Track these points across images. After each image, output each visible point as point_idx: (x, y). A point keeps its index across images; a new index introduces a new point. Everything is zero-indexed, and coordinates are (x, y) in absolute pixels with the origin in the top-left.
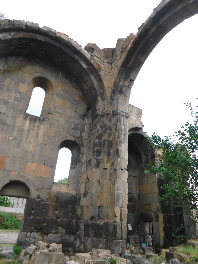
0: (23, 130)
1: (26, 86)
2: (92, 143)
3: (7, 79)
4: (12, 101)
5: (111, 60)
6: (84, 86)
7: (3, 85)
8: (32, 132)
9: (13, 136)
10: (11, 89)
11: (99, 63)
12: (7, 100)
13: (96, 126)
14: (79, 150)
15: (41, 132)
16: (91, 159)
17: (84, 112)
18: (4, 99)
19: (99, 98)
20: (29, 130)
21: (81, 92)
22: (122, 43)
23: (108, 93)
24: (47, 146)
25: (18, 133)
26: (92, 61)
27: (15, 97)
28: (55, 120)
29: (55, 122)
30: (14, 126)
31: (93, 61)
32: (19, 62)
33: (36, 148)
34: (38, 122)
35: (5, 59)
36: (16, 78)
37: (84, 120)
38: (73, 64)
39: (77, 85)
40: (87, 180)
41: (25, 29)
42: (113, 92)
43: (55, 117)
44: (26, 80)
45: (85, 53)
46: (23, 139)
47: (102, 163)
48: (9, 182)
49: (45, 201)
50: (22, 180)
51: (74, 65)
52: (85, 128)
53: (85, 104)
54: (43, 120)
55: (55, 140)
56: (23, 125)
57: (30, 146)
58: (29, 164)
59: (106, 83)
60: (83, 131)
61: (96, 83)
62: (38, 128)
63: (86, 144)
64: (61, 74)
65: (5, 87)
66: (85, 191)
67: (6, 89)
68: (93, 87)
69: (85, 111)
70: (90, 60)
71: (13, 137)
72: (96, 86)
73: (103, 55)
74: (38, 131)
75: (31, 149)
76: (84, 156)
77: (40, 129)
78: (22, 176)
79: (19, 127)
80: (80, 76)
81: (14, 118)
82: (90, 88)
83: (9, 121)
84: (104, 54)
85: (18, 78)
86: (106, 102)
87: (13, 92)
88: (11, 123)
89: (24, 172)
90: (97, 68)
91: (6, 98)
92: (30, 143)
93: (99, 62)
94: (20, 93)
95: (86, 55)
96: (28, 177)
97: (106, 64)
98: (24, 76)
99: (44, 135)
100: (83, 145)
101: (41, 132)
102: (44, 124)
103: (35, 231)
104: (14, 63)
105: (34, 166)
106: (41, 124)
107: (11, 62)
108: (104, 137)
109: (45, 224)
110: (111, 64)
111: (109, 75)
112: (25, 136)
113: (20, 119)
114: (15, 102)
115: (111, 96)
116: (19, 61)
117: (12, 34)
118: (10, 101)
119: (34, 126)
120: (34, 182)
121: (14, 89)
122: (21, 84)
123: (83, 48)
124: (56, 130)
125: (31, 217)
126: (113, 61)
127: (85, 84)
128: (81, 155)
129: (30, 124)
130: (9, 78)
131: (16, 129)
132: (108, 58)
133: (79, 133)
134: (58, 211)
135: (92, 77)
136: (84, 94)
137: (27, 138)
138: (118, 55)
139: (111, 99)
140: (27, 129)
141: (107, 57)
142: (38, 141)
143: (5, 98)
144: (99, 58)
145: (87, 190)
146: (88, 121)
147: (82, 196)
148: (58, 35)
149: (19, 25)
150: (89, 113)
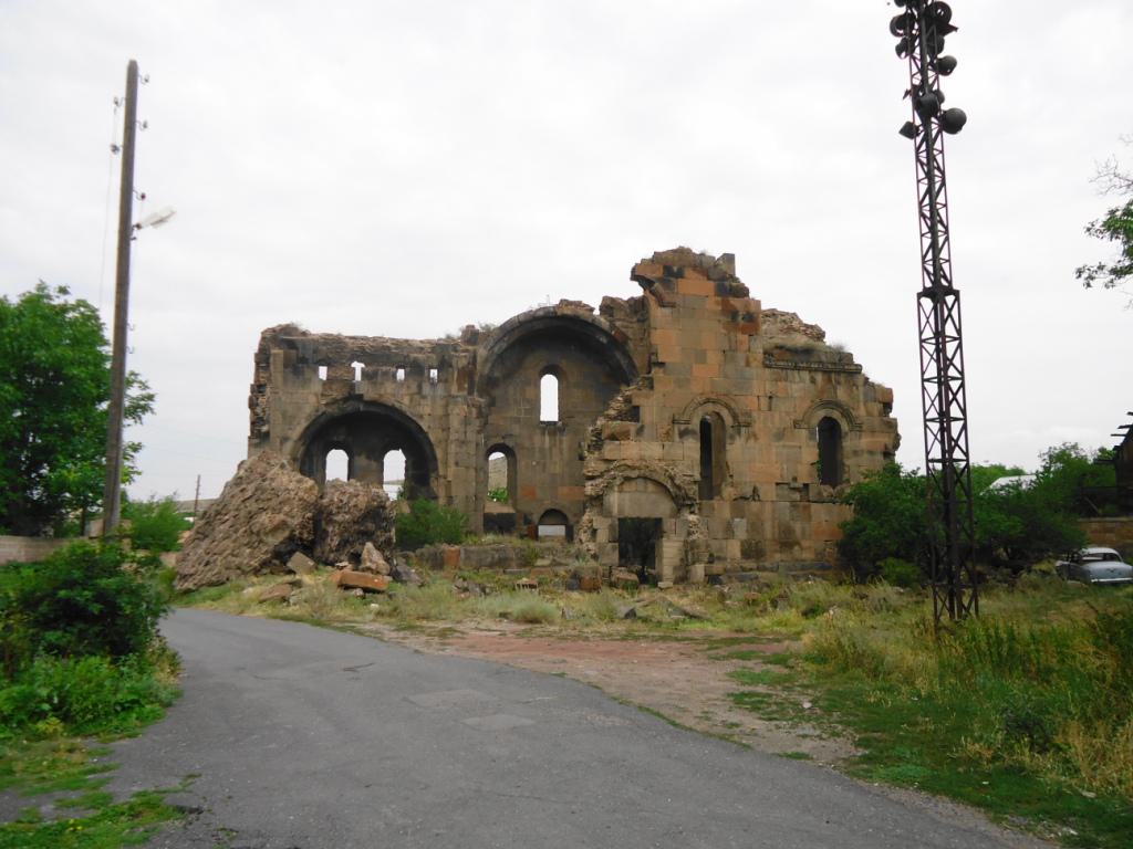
5: (642, 315)
11: (624, 330)
15: (565, 446)
20: (551, 449)
30: (533, 448)
45: (600, 322)
50: (557, 507)
56: (543, 442)
61: (624, 362)
62: (561, 442)
64: (573, 347)
68: (620, 367)
72: (625, 367)
75: (558, 469)
83: (527, 444)
92: (555, 463)
97: (635, 325)
101: (565, 446)
105: (564, 490)
117: (506, 339)
123: (597, 312)
135: (618, 355)
137: (551, 458)
141: (636, 312)
144: (624, 320)
148: (559, 313)
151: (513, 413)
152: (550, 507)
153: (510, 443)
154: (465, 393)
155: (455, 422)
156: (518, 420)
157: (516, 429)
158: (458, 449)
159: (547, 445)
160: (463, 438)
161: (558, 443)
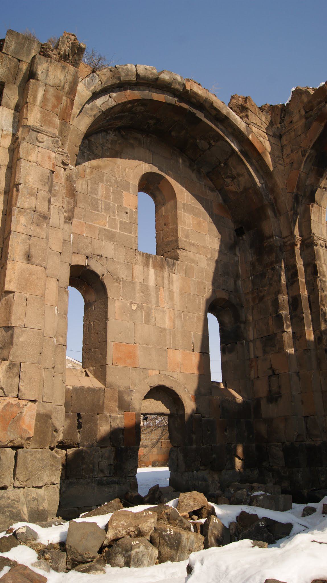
0: (147, 287)
1: (132, 195)
2: (269, 303)
3: (101, 185)
4: (118, 231)
6: (228, 185)
7: (97, 199)
8: (162, 289)
9: (138, 303)
10: (111, 205)
11: (261, 139)
12: (111, 229)
13: (273, 269)
14: (237, 318)
15: (176, 287)
16: (275, 332)
17: (232, 236)
18: (105, 230)
19: (270, 212)
20: (157, 287)
21: (219, 195)
22: (305, 99)
23: (285, 200)
24: (190, 314)
25: (142, 294)
26: (250, 137)
27: (121, 222)
28: (193, 261)
29: (193, 264)
30: (133, 283)
31: (252, 136)
32: (110, 146)
33: (174, 320)
34: (167, 268)
35: (87, 142)
36: (113, 182)
37: (235, 254)
38: (212, 141)
39: (211, 180)
40: (270, 372)
41: (134, 82)
42: (296, 199)
43: (190, 254)
44: (128, 184)
46: (153, 307)
47: (298, 340)
48: (149, 390)
49: (207, 416)
50: (168, 384)
51: (213, 144)
52: (238, 270)
53: (230, 221)
54: (174, 264)
55: (199, 302)
56: (146, 278)
57: (165, 319)
58: (171, 353)
59: (280, 182)
60: (237, 277)
63: (251, 304)
64: (181, 161)
65: (102, 203)
66: (270, 391)
67: (103, 207)
69: (234, 236)
70: (246, 133)
71: (136, 304)
73: (264, 120)
74: (171, 288)
75: (167, 324)
76: (251, 328)
77: (172, 282)
78: (166, 377)
79: (142, 284)
80: (222, 165)
81: (129, 265)
82: (246, 190)
83: (123, 274)
84: (266, 118)
85: (116, 182)
86: (282, 218)
87: (116, 213)
88: (127, 276)
89: (167, 369)
90: (260, 151)
91: (107, 226)
93: (261, 136)
94: (127, 213)
95: (239, 123)
96: (175, 376)
98: (124, 174)
99: (182, 294)
100: (242, 306)
101: (176, 287)
102: (176, 271)
103: (202, 468)
104: (102, 148)
106: (172, 272)
107: (97, 147)
108: (291, 290)
109: (214, 456)
110: (280, 137)
111: (280, 162)
112: (153, 299)
113: (139, 266)
114: (124, 233)
115: (293, 209)
116: (111, 144)
118: (116, 231)
119: (163, 277)
120: (186, 386)
121: (116, 205)
122: (124, 192)
124: (197, 281)
125: (194, 446)
126: (285, 133)
127: (232, 181)
128: (242, 325)
129: (156, 274)
130: (103, 182)
131: (138, 287)
132: (273, 125)
133: (232, 281)
134: (227, 431)
136: (225, 201)
137: (157, 304)
138: (295, 120)
139: (294, 213)
140: (154, 285)
142: (175, 306)
143: (107, 227)
145: (274, 388)
146: (245, 257)
147: (263, 403)
148: (188, 88)
149: (127, 75)
150: (243, 239)
151: (104, 223)
152: (156, 382)
153: (97, 267)
154: (56, 132)
155: (30, 175)
156: (110, 236)
157: (108, 249)
158: (34, 229)
159: (152, 281)
160: (43, 207)
161: (166, 281)
